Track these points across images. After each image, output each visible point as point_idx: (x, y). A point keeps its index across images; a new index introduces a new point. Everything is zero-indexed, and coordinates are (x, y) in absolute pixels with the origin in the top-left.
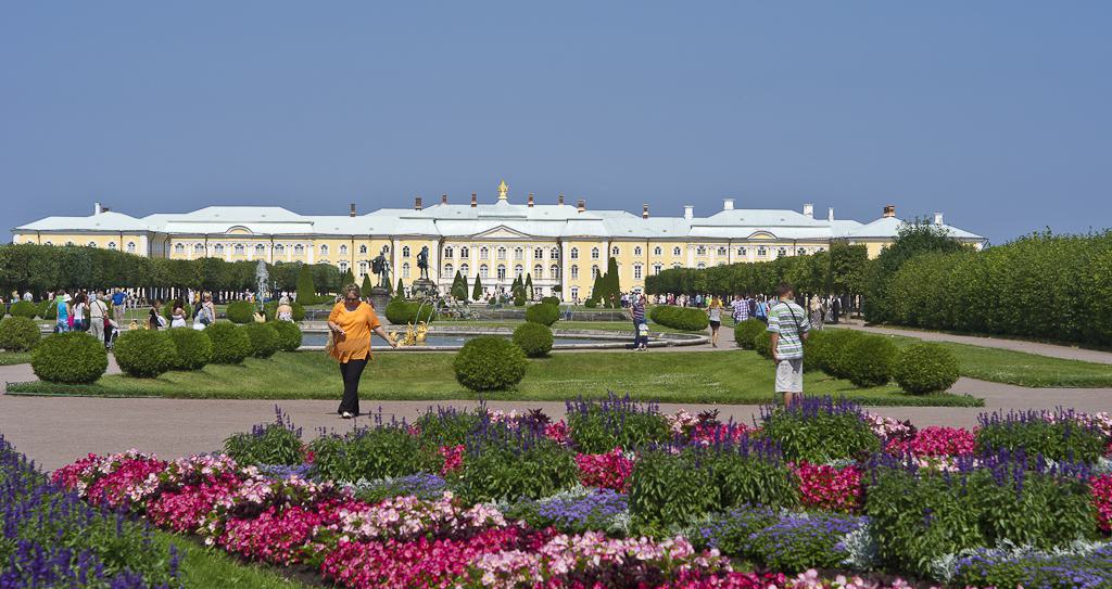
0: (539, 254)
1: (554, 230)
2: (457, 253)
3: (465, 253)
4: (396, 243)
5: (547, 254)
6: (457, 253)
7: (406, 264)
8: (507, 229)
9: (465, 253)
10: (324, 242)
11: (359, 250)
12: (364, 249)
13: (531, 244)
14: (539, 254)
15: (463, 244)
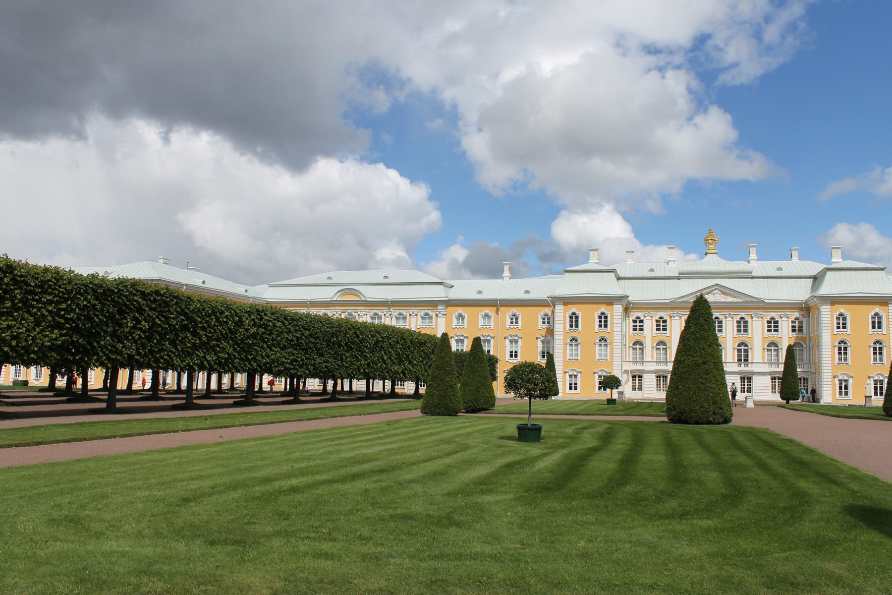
0: (773, 325)
1: (800, 292)
2: (649, 325)
3: (661, 325)
4: (559, 309)
5: (785, 326)
6: (649, 325)
7: (603, 339)
8: (725, 291)
9: (661, 325)
10: (460, 310)
11: (509, 321)
12: (515, 318)
13: (761, 312)
14: (773, 325)
15: (658, 315)
